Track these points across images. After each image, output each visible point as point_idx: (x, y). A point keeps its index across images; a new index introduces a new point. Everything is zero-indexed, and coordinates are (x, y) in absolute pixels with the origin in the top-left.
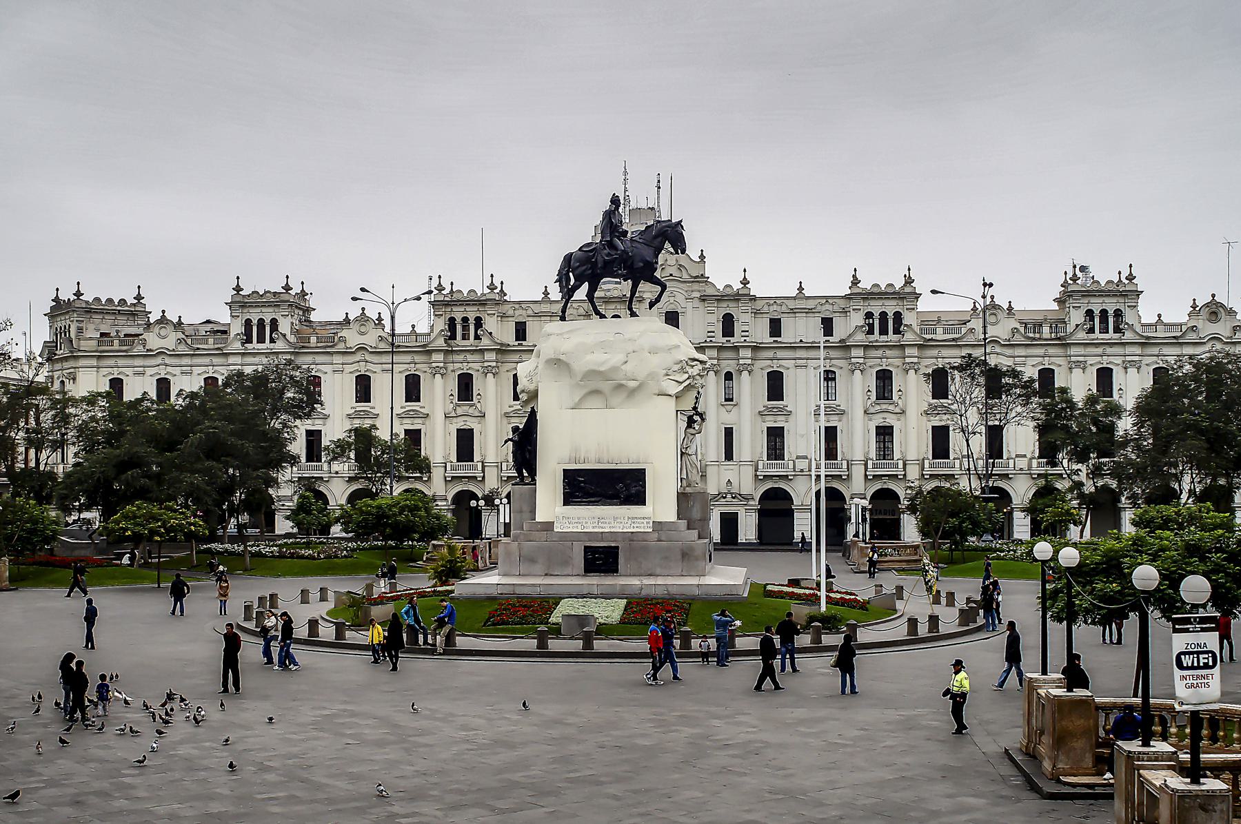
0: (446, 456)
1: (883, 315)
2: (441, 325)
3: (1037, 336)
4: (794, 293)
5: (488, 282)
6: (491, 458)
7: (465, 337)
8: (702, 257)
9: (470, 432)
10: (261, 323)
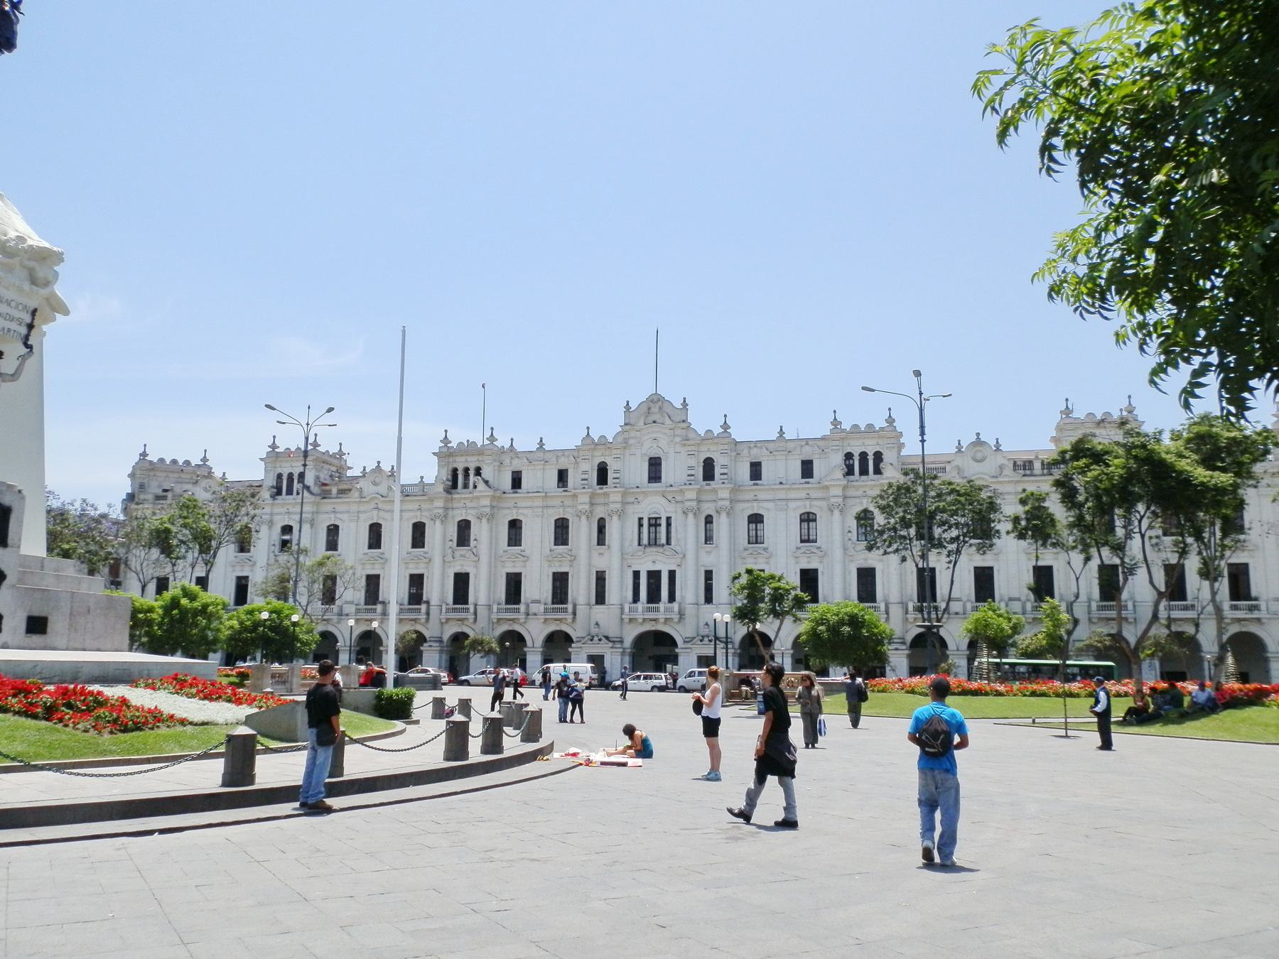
0: (443, 600)
1: (863, 456)
2: (446, 475)
3: (1028, 472)
4: (774, 436)
5: (488, 434)
6: (482, 600)
7: (466, 486)
8: (685, 404)
9: (467, 575)
10: (290, 476)
